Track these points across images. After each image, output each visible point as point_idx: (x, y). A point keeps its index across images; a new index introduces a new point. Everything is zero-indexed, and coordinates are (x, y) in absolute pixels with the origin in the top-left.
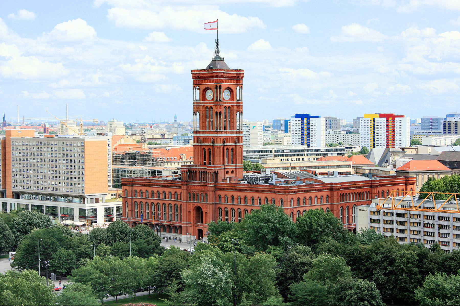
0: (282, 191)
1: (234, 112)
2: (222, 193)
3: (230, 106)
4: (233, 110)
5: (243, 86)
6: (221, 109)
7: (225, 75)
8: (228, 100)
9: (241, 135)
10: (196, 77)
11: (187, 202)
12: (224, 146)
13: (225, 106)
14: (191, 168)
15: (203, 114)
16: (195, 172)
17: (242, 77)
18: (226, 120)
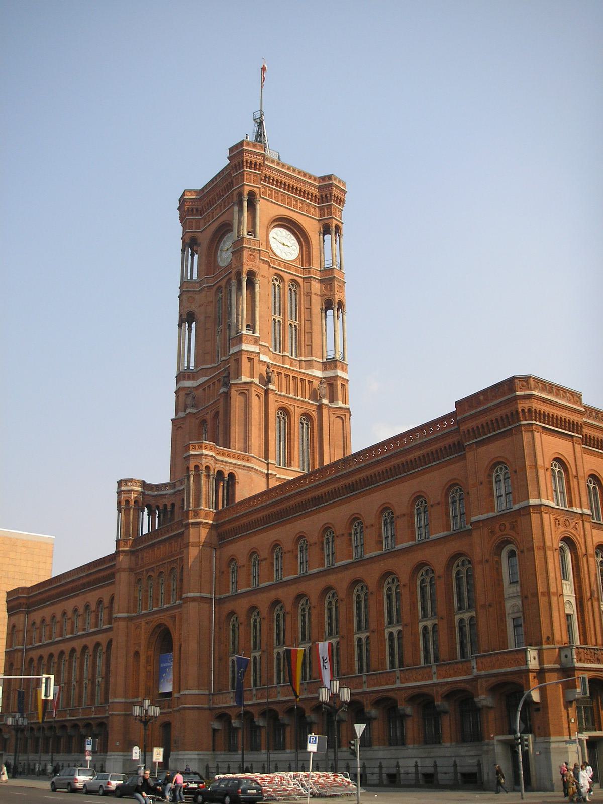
0: (498, 413)
1: (313, 301)
2: (239, 549)
3: (300, 281)
4: (308, 295)
5: (344, 228)
6: (253, 263)
7: (274, 175)
8: (293, 261)
9: (340, 373)
10: (191, 211)
11: (129, 619)
12: (267, 392)
13: (277, 275)
14: (156, 496)
15: (206, 314)
16: (169, 508)
17: (341, 201)
18: (284, 319)
